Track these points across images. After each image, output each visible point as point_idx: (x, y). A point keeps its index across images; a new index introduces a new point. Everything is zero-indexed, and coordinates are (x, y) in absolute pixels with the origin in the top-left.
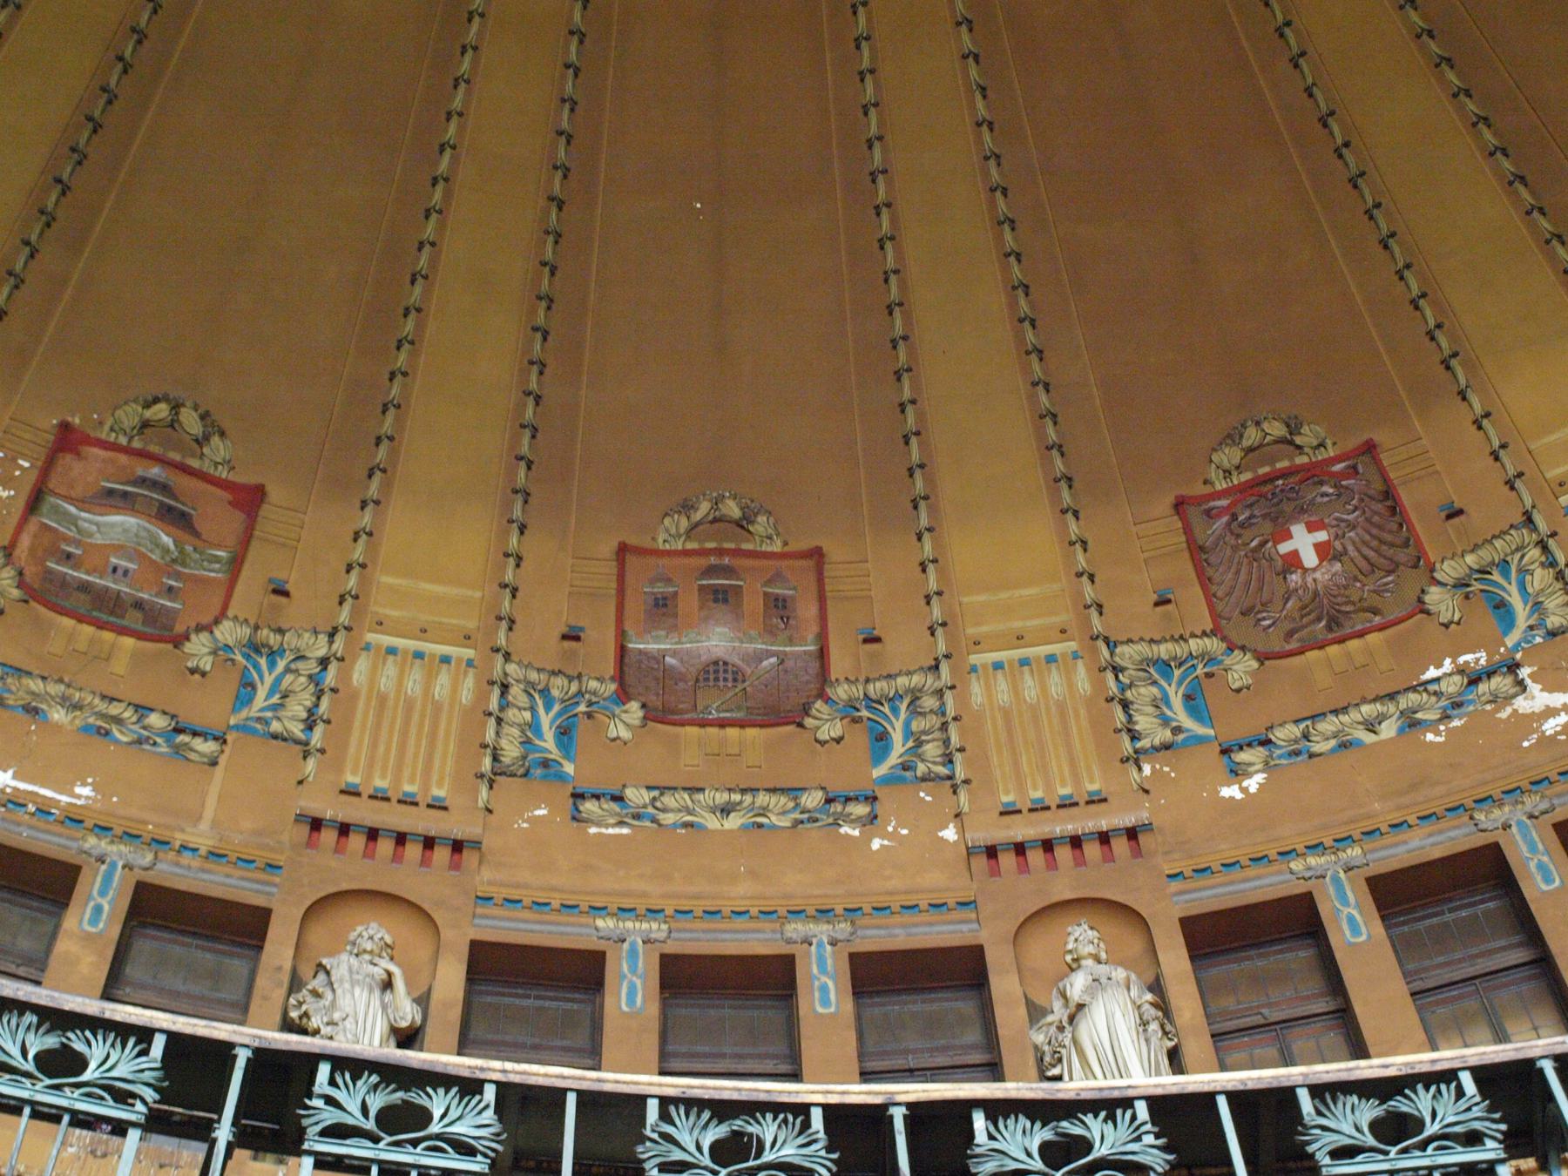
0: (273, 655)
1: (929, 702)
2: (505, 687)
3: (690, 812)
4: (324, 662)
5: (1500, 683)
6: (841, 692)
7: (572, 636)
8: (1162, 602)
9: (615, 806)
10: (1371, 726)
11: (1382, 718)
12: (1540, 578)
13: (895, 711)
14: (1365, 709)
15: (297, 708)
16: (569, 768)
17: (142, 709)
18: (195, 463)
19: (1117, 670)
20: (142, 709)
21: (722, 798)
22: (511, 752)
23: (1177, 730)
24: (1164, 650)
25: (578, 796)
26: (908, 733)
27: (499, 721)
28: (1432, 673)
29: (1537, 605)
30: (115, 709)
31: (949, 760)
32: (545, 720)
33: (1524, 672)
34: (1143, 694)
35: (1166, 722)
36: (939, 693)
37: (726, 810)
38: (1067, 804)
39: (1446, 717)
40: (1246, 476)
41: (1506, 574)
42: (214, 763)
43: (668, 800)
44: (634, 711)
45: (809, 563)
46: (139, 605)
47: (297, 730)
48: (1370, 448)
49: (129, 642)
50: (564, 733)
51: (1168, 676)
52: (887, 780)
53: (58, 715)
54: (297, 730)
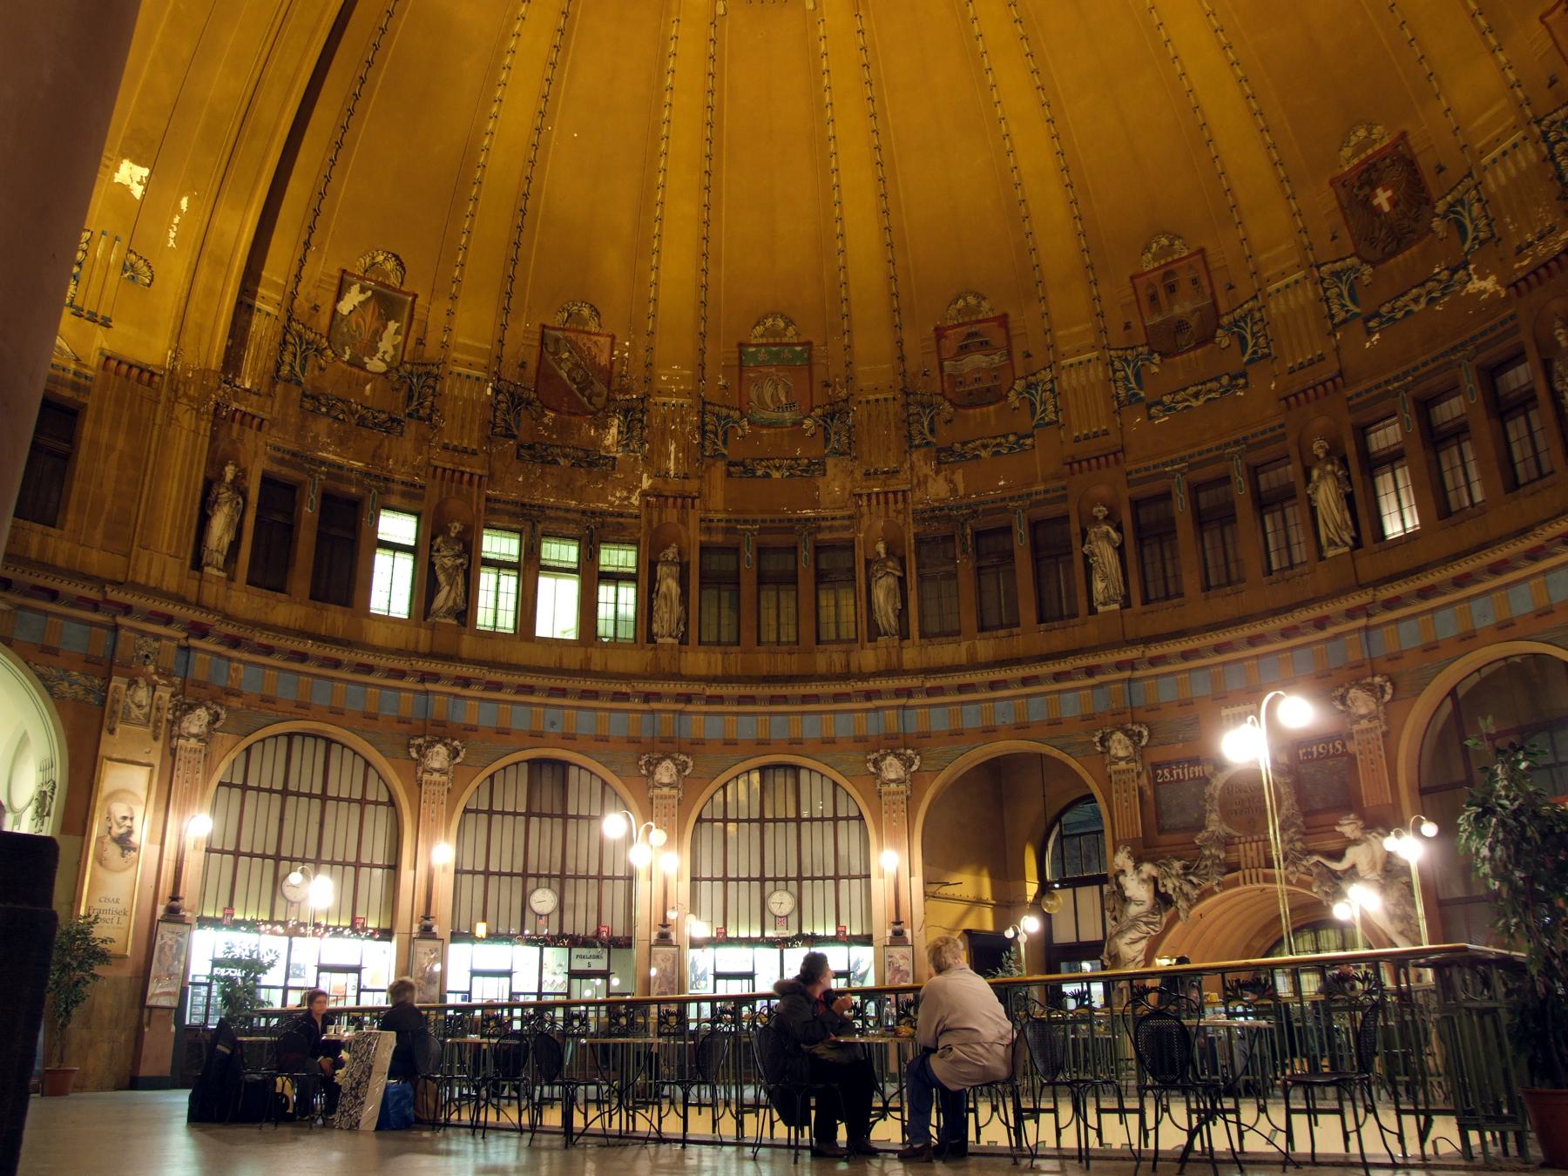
0: (1035, 385)
1: (1257, 315)
2: (1112, 364)
3: (1187, 400)
4: (1052, 381)
5: (1461, 273)
6: (1225, 320)
7: (1127, 326)
8: (1334, 238)
9: (1159, 407)
10: (1416, 300)
11: (1420, 296)
12: (1476, 207)
13: (1246, 323)
14: (1414, 291)
15: (1050, 408)
16: (1142, 394)
17: (1005, 436)
18: (980, 317)
19: (1323, 280)
20: (1005, 436)
21: (1192, 390)
22: (1122, 393)
23: (1347, 311)
24: (1338, 266)
25: (1149, 407)
26: (1253, 335)
27: (1115, 381)
28: (1437, 270)
29: (1476, 228)
30: (998, 440)
31: (1268, 347)
32: (1129, 372)
33: (1471, 267)
34: (1333, 292)
35: (1343, 306)
36: (1260, 310)
37: (1196, 395)
38: (1311, 362)
39: (1443, 295)
40: (1356, 161)
41: (1463, 207)
42: (1034, 447)
43: (1179, 397)
44: (1157, 358)
45: (1199, 256)
46: (988, 390)
47: (1053, 416)
48: (1403, 135)
49: (992, 408)
50: (1137, 376)
51: (1341, 281)
52: (1251, 361)
53: (983, 454)
54: (1053, 416)
